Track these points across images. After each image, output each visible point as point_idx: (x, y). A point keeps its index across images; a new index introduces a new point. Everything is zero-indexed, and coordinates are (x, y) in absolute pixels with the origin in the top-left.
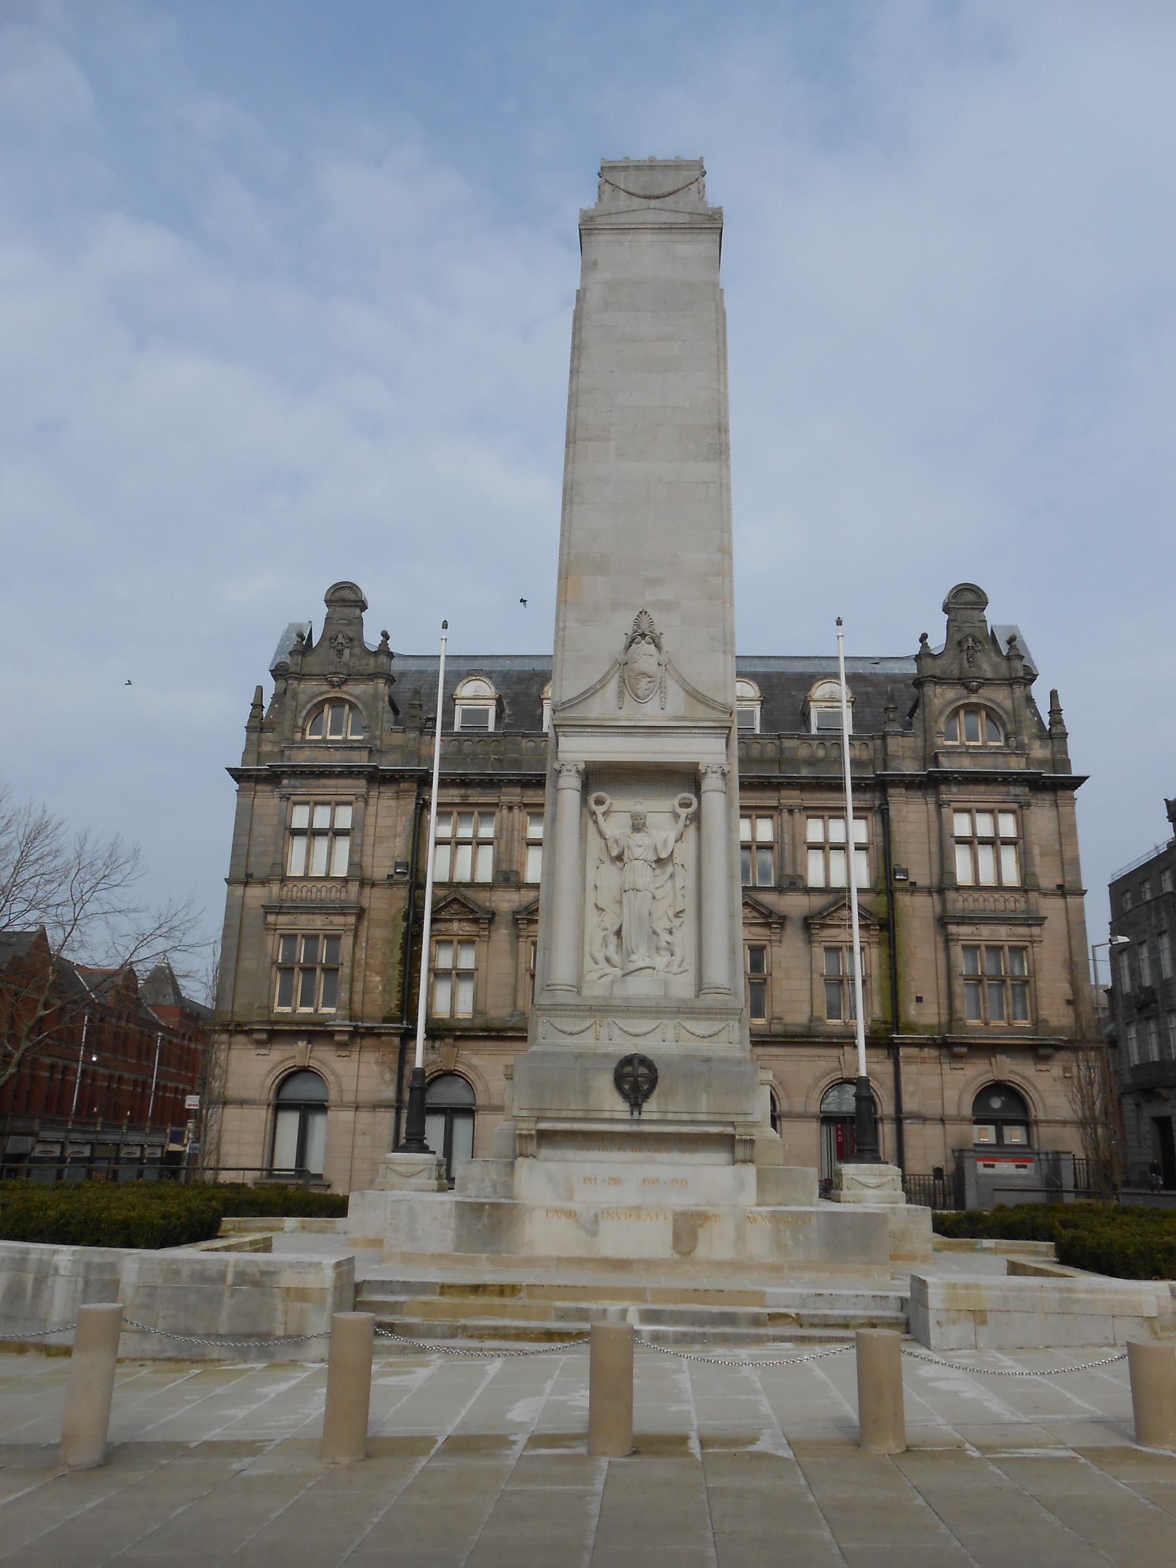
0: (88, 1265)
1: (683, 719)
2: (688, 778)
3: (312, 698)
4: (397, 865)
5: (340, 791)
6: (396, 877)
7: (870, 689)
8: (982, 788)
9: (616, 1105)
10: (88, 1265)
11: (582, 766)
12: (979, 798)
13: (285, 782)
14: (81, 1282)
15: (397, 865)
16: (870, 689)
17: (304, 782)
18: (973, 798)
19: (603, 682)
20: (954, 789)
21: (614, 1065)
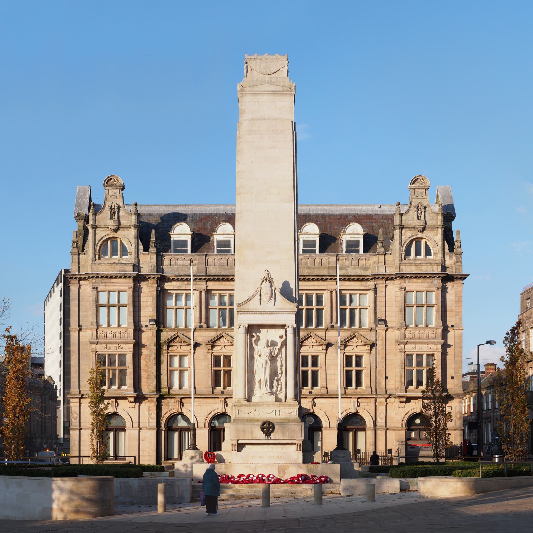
0: (120, 482)
1: (281, 309)
2: (283, 327)
3: (102, 238)
4: (150, 320)
5: (121, 285)
6: (150, 326)
7: (374, 224)
8: (419, 280)
9: (262, 435)
10: (120, 482)
11: (247, 326)
12: (418, 285)
13: (94, 281)
14: (119, 486)
15: (150, 320)
16: (374, 224)
17: (103, 281)
18: (415, 285)
19: (254, 296)
20: (407, 281)
21: (260, 423)
